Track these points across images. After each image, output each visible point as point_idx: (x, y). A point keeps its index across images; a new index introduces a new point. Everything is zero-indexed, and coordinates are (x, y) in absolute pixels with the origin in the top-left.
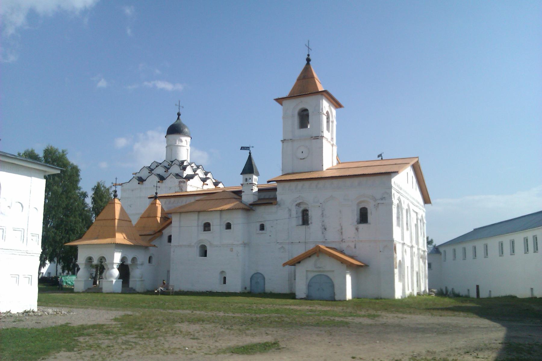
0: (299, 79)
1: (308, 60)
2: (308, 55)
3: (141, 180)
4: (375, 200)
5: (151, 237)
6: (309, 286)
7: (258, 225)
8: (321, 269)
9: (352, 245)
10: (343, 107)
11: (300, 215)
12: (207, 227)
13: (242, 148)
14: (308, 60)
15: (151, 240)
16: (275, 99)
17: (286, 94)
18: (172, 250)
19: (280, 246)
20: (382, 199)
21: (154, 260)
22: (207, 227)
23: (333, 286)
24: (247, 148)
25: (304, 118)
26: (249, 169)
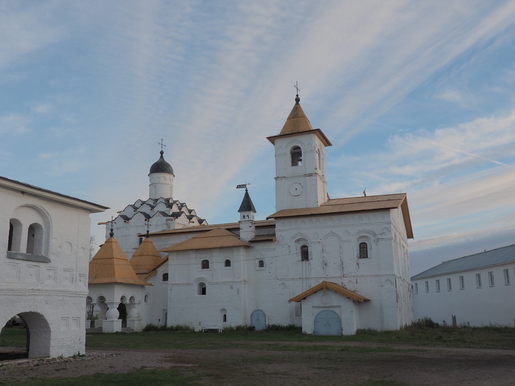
1: (297, 100)
2: (297, 96)
3: (126, 219)
5: (145, 276)
6: (315, 322)
7: (257, 262)
8: (328, 305)
9: (354, 280)
10: (331, 145)
11: (299, 251)
12: (205, 265)
14: (297, 100)
15: (146, 279)
16: (267, 138)
17: (277, 133)
18: (169, 288)
19: (280, 282)
21: (149, 299)
22: (205, 265)
23: (340, 321)
24: (244, 186)
25: (296, 155)
26: (247, 206)
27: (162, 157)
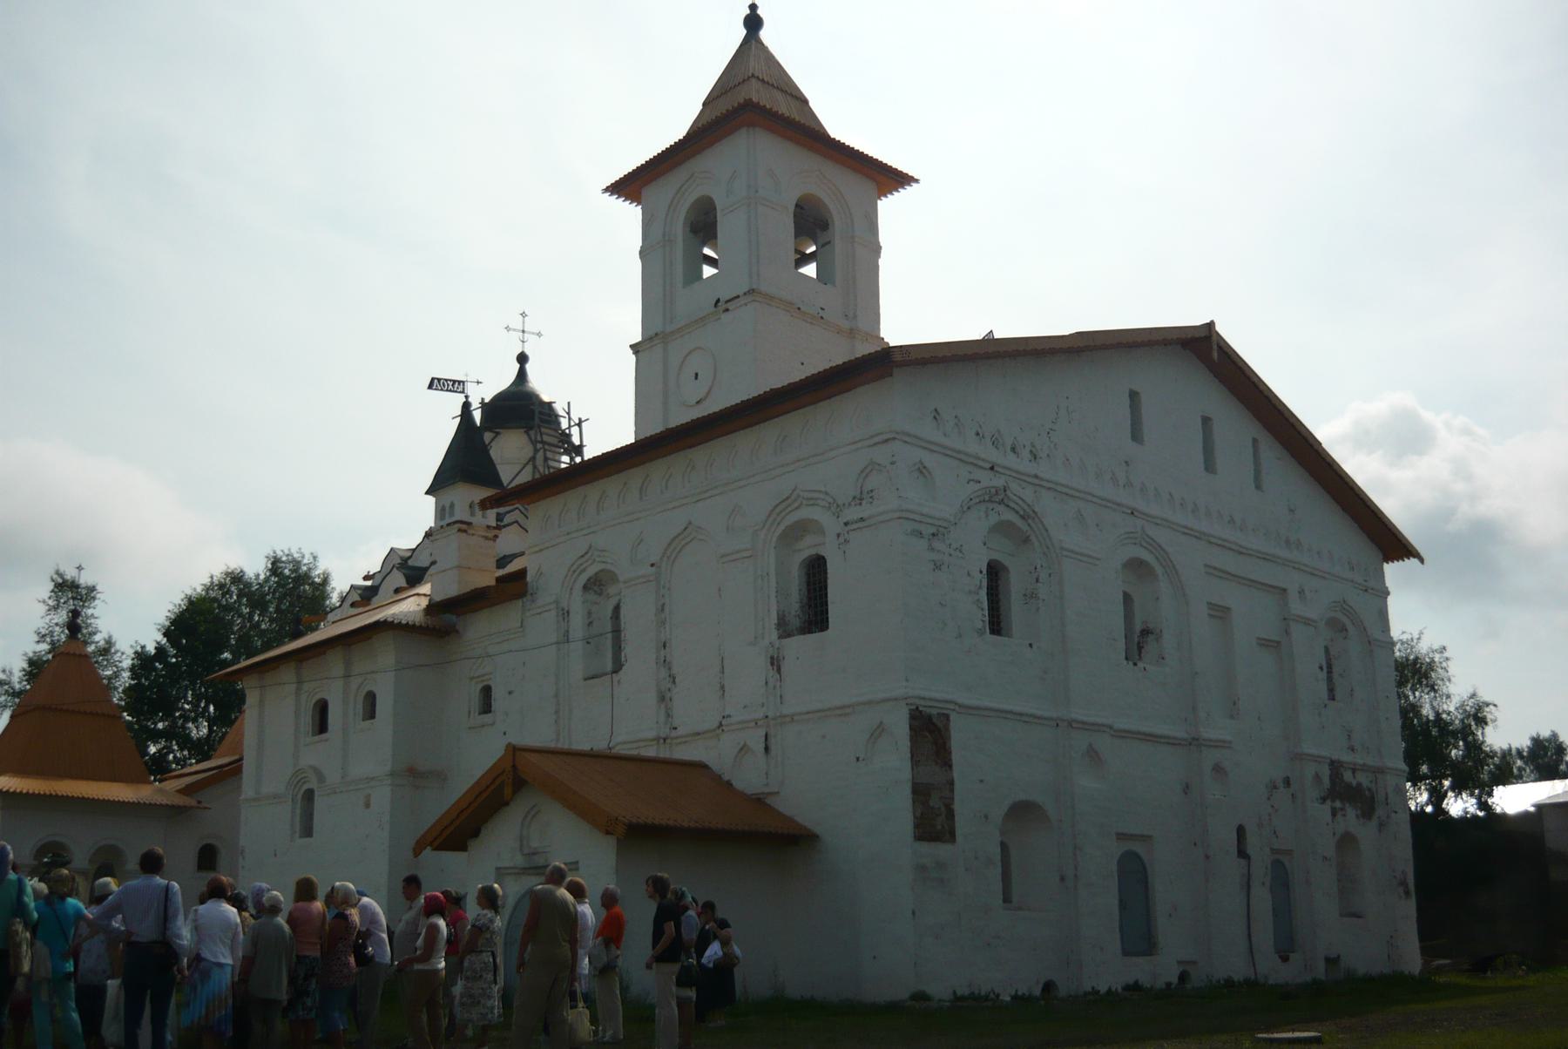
0: (704, 104)
2: (753, 7)
9: (755, 740)
16: (607, 190)
27: (522, 375)
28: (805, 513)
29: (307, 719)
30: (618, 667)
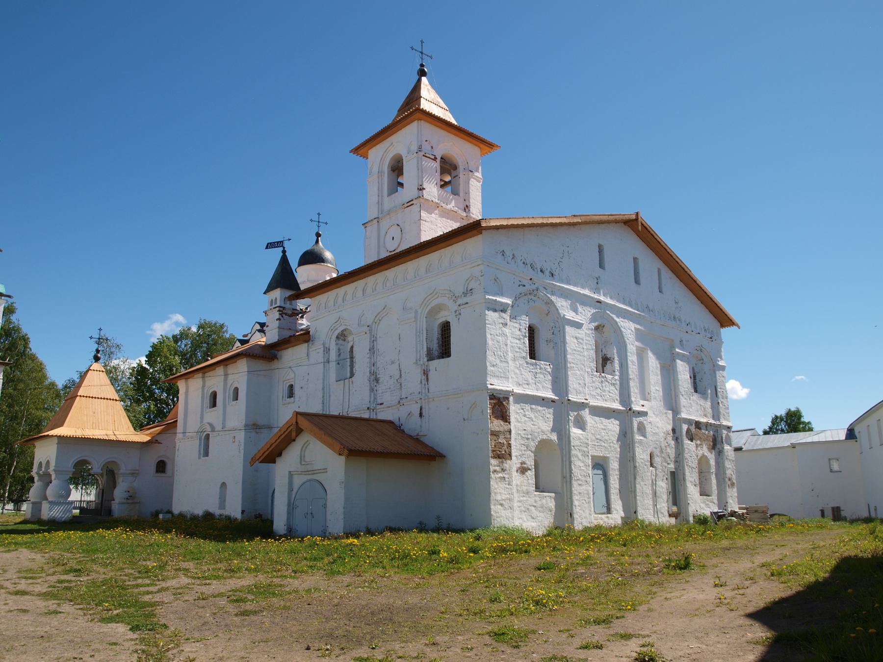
2: (422, 65)
4: (455, 298)
8: (309, 468)
13: (270, 246)
16: (351, 152)
20: (465, 294)
24: (279, 244)
28: (439, 301)
29: (207, 401)
30: (352, 375)
